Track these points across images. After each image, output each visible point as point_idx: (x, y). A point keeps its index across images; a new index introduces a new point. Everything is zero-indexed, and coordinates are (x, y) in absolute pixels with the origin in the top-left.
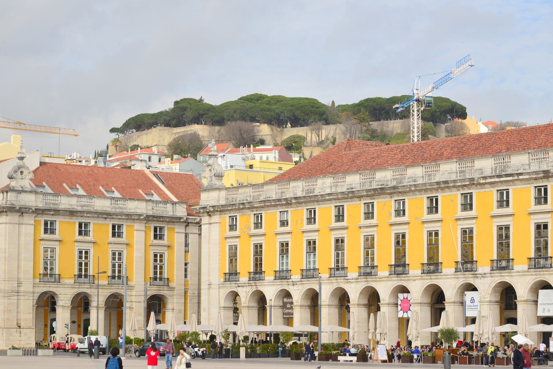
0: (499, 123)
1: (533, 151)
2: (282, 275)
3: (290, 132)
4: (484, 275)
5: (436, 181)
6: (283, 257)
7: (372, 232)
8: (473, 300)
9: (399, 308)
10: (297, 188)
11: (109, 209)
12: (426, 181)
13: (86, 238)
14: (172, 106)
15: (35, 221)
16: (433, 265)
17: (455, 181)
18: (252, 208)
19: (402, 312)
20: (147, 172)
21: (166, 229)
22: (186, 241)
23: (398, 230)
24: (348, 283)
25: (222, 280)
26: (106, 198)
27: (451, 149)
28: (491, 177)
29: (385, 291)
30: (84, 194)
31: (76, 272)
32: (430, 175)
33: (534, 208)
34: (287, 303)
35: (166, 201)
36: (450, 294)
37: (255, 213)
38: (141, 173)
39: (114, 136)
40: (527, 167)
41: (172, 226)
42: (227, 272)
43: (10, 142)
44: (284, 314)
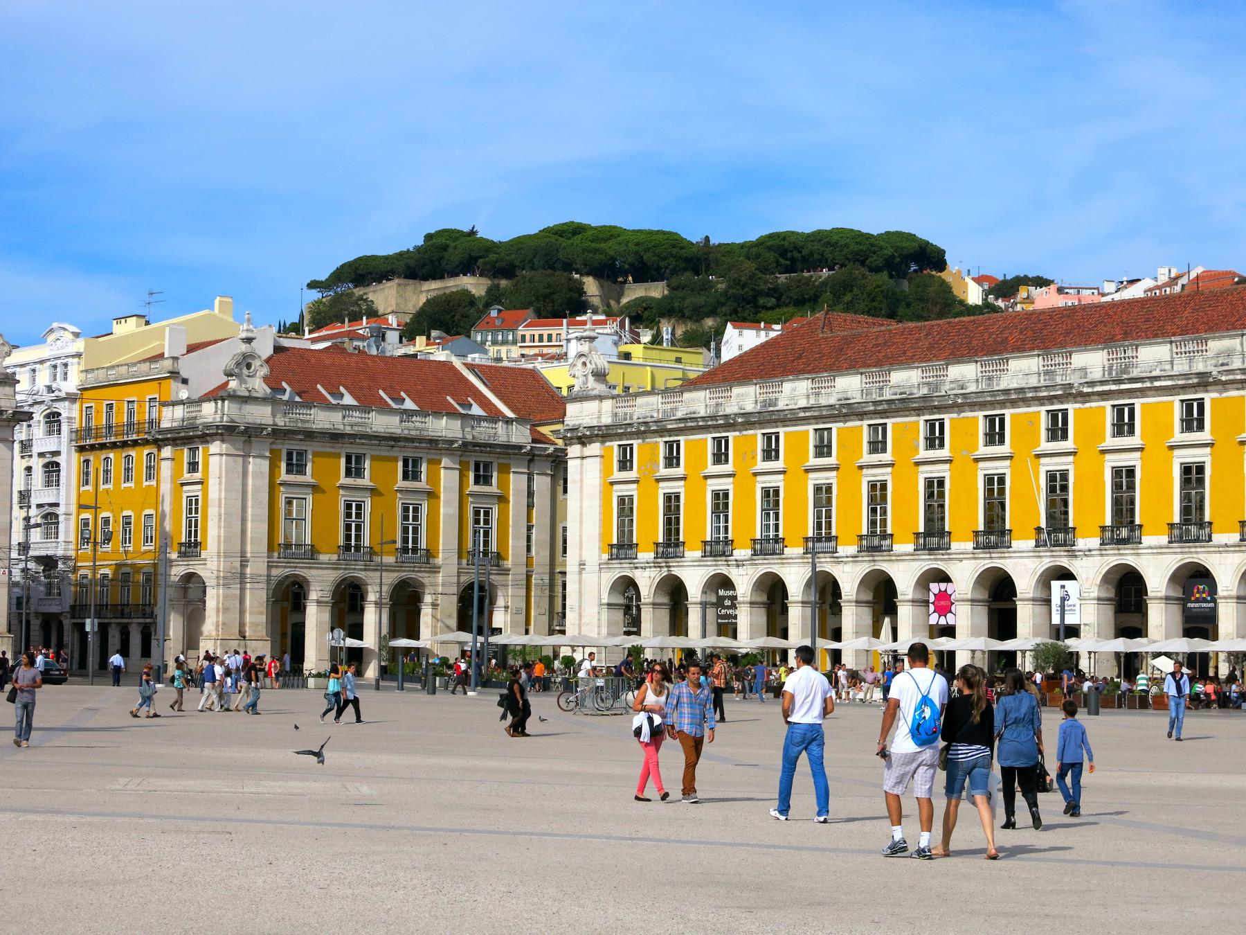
0: (1001, 278)
1: (1178, 338)
2: (718, 548)
4: (1088, 553)
5: (1002, 387)
6: (719, 517)
7: (883, 475)
9: (932, 608)
11: (399, 431)
12: (983, 386)
13: (359, 482)
14: (420, 242)
15: (271, 451)
16: (995, 532)
17: (1036, 389)
18: (662, 432)
19: (936, 615)
20: (457, 363)
21: (495, 466)
22: (529, 487)
23: (931, 472)
24: (839, 563)
25: (606, 556)
26: (392, 411)
27: (1021, 332)
28: (1102, 383)
29: (905, 577)
30: (354, 403)
31: (341, 542)
32: (990, 379)
33: (1179, 437)
34: (724, 598)
35: (494, 416)
36: (1025, 584)
37: (667, 439)
38: (447, 365)
39: (315, 295)
40: (1168, 367)
41: (506, 461)
42: (615, 542)
43: (212, 308)
44: (719, 617)
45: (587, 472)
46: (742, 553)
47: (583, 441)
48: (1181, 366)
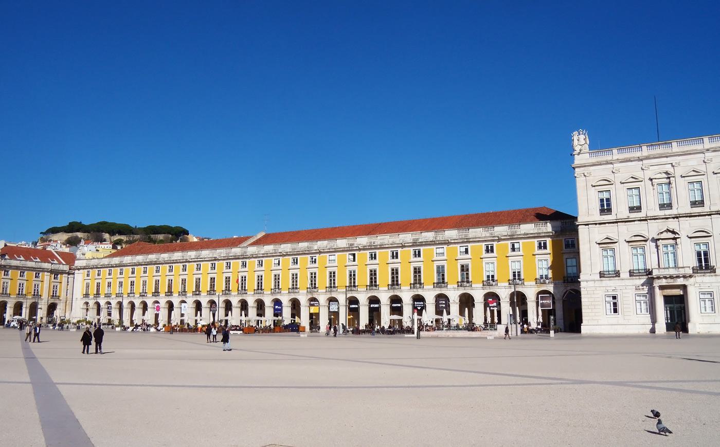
2: (108, 295)
3: (117, 237)
8: (185, 307)
10: (116, 260)
14: (68, 224)
16: (170, 292)
17: (180, 260)
18: (97, 268)
20: (53, 251)
26: (34, 262)
28: (194, 259)
29: (150, 302)
31: (17, 293)
35: (60, 263)
36: (176, 304)
39: (42, 235)
45: (79, 276)
46: (113, 296)
47: (79, 269)
48: (211, 256)
